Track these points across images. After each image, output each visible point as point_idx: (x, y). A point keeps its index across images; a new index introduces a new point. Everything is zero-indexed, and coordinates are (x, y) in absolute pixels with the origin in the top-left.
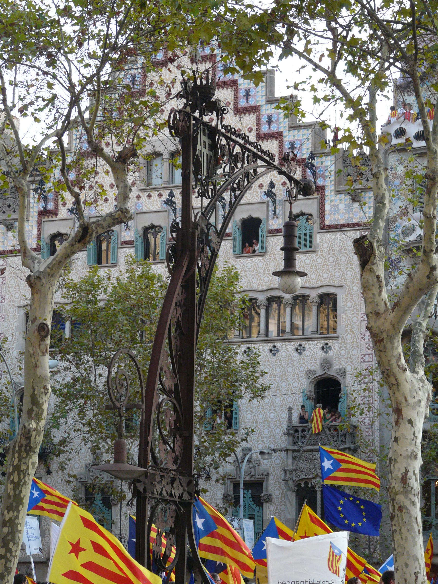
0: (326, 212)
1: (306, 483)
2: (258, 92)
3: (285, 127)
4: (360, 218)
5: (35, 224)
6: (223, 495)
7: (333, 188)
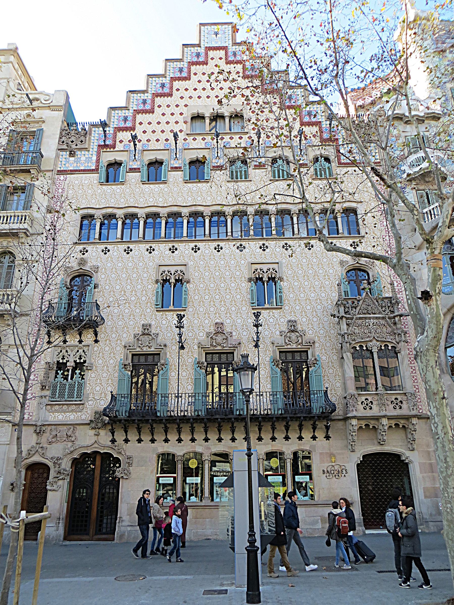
1: (361, 347)
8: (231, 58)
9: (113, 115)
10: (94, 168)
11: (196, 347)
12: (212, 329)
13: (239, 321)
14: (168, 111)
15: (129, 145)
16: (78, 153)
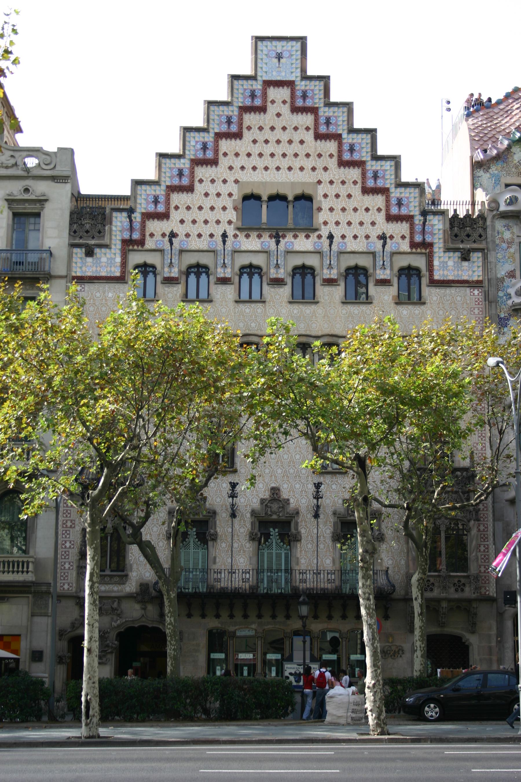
0: (436, 268)
2: (363, 148)
3: (391, 184)
4: (469, 276)
5: (118, 252)
6: (333, 533)
7: (441, 245)
8: (299, 103)
9: (139, 192)
10: (118, 274)
11: (248, 515)
12: (267, 495)
13: (297, 486)
14: (212, 190)
15: (163, 241)
16: (97, 250)
